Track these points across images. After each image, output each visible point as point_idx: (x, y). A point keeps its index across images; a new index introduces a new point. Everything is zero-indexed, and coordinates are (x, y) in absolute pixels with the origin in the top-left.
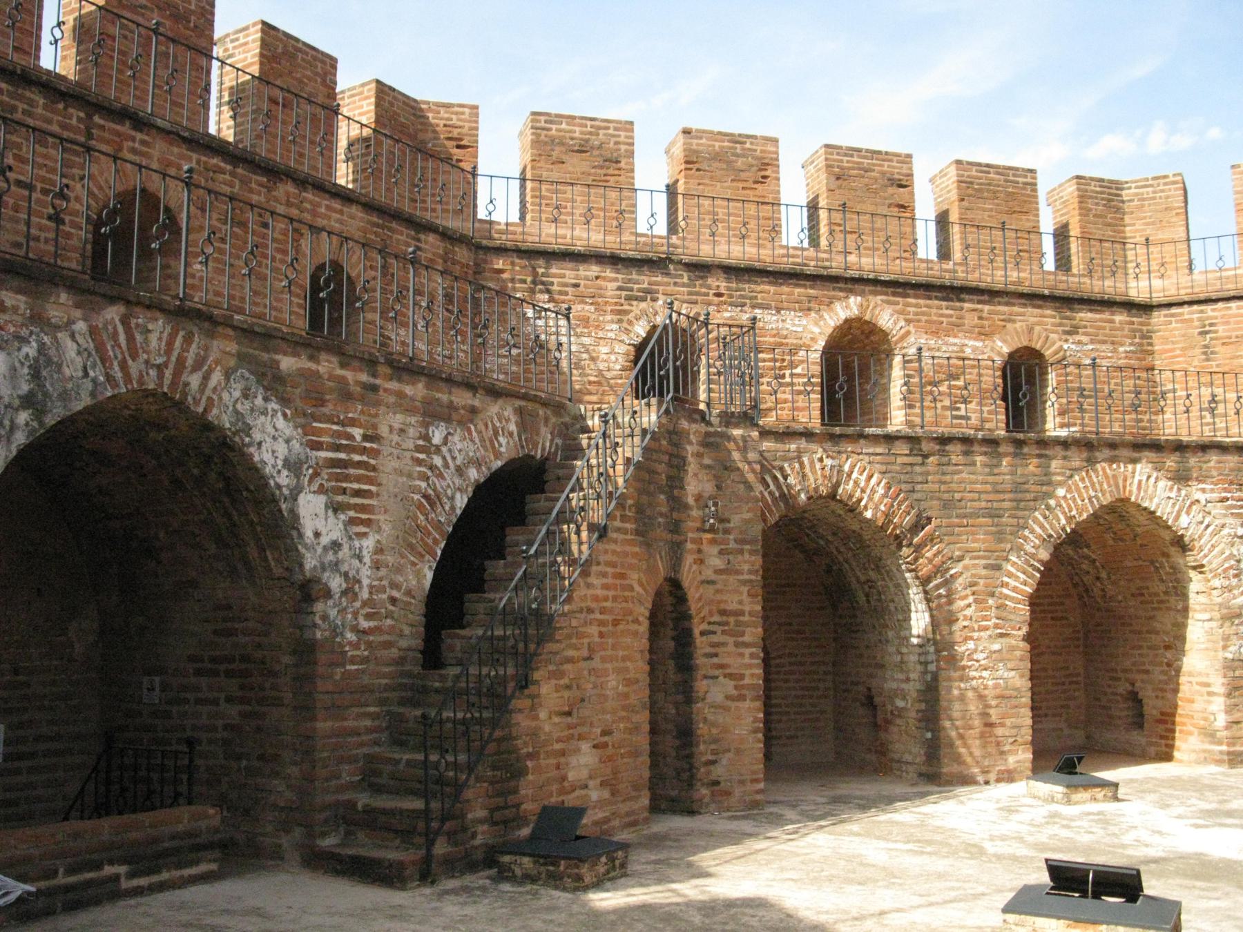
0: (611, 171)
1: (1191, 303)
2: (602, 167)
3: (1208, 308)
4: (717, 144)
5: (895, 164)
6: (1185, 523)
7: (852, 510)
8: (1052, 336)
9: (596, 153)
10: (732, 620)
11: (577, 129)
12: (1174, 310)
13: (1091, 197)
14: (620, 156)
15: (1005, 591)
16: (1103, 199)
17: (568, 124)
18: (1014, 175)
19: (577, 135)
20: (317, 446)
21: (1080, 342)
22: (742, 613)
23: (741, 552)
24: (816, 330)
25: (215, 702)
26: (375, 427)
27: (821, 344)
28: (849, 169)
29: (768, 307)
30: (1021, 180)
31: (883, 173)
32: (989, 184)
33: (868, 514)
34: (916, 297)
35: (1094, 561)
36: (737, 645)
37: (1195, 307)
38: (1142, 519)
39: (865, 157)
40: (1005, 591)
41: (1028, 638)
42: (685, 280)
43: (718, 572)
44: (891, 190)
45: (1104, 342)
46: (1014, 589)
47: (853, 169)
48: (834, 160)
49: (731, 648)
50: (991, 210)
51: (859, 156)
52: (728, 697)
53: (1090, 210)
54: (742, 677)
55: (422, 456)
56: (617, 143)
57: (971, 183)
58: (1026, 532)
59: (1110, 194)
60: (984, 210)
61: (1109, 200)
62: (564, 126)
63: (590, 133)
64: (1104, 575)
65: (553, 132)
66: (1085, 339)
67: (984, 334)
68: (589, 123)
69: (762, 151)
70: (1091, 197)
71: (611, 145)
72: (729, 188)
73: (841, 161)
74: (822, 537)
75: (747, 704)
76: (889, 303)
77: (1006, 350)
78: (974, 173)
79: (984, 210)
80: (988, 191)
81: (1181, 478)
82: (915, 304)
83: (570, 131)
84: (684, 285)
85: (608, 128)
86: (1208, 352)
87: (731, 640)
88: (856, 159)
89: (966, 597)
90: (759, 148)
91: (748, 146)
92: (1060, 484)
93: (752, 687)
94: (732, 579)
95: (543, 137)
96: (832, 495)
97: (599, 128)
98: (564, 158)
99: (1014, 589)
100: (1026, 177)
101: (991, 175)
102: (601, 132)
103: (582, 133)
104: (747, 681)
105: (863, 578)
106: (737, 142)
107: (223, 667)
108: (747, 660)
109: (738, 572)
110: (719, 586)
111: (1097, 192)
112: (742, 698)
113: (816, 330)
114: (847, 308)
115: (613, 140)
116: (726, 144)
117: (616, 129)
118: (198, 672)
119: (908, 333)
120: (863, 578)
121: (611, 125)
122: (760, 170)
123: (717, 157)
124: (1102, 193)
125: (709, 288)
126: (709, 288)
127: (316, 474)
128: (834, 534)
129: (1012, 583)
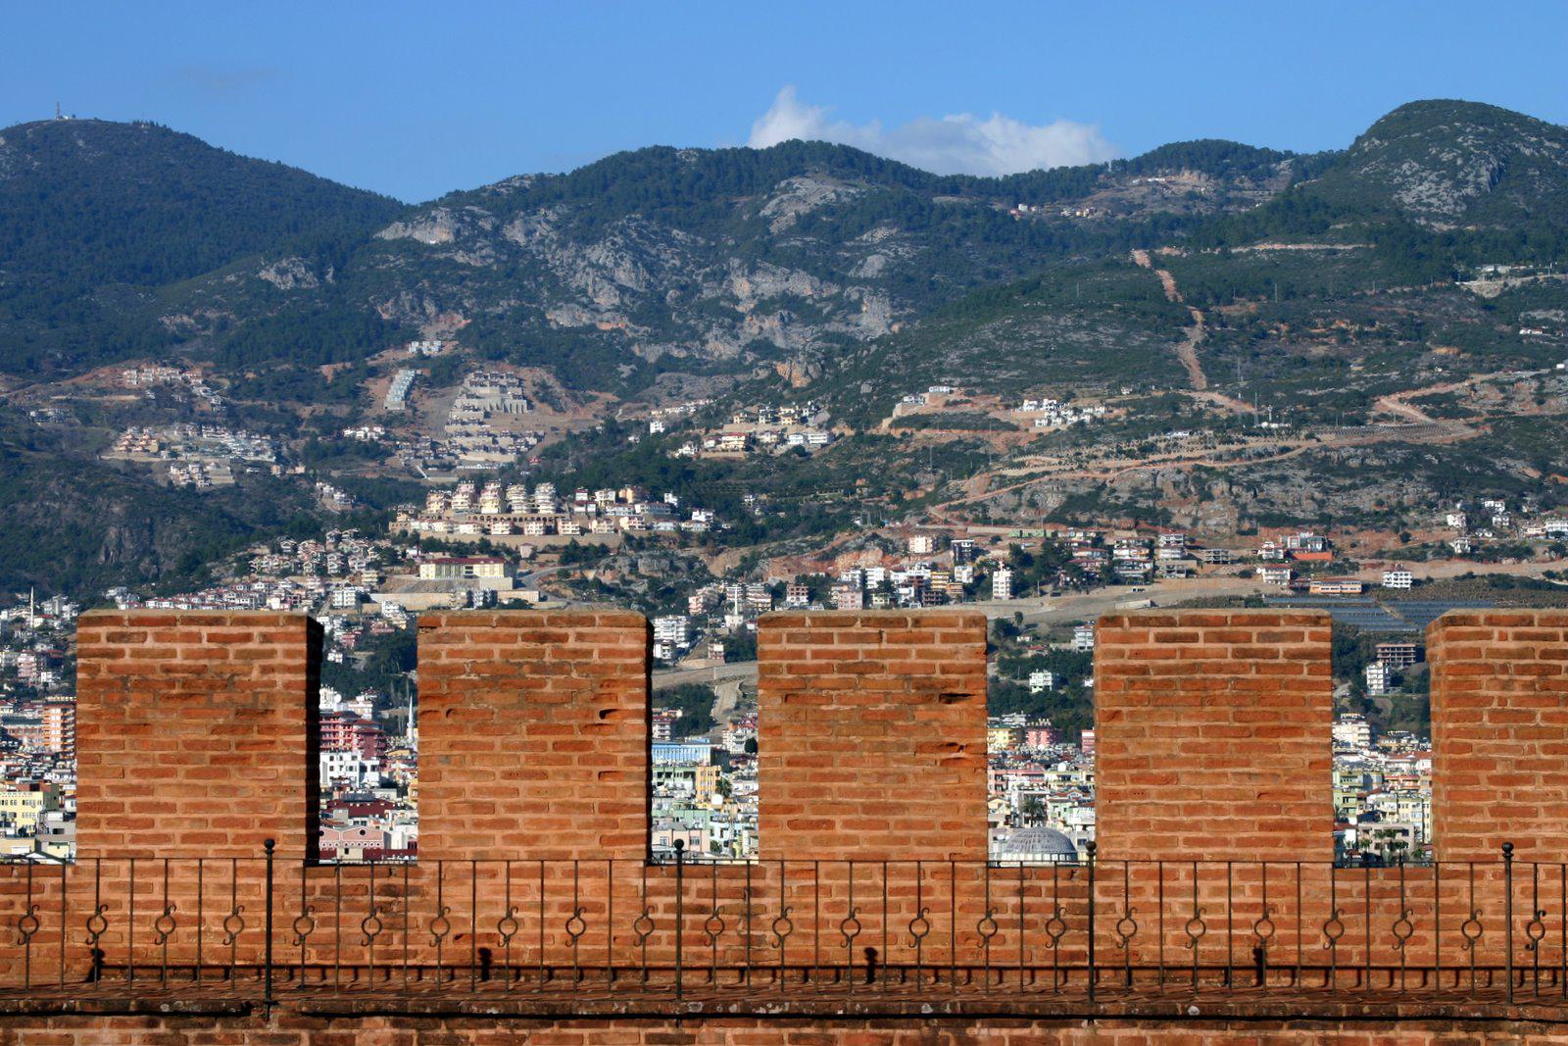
0: (256, 737)
2: (233, 730)
4: (497, 648)
5: (938, 646)
9: (219, 697)
11: (179, 647)
13: (1489, 669)
14: (271, 697)
16: (1523, 670)
17: (158, 637)
18: (1263, 637)
19: (178, 661)
28: (819, 670)
30: (1281, 647)
31: (905, 675)
32: (1193, 668)
39: (862, 638)
44: (923, 712)
47: (828, 669)
48: (782, 655)
50: (1194, 730)
51: (846, 638)
53: (1489, 700)
56: (265, 670)
57: (1144, 670)
59: (1545, 654)
60: (1174, 732)
61: (1544, 671)
62: (150, 644)
63: (209, 654)
65: (127, 660)
68: (205, 631)
69: (603, 653)
70: (1489, 669)
71: (255, 675)
72: (524, 746)
73: (800, 655)
78: (1152, 645)
79: (1174, 732)
80: (1186, 684)
83: (166, 654)
85: (248, 638)
88: (836, 646)
90: (596, 647)
91: (572, 644)
95: (103, 675)
97: (228, 639)
98: (152, 716)
100: (1299, 637)
101: (1200, 645)
102: (232, 648)
103: (188, 655)
106: (543, 638)
111: (1509, 654)
115: (257, 663)
116: (520, 645)
117: (266, 638)
121: (255, 631)
122: (596, 699)
123: (499, 679)
124: (1521, 654)
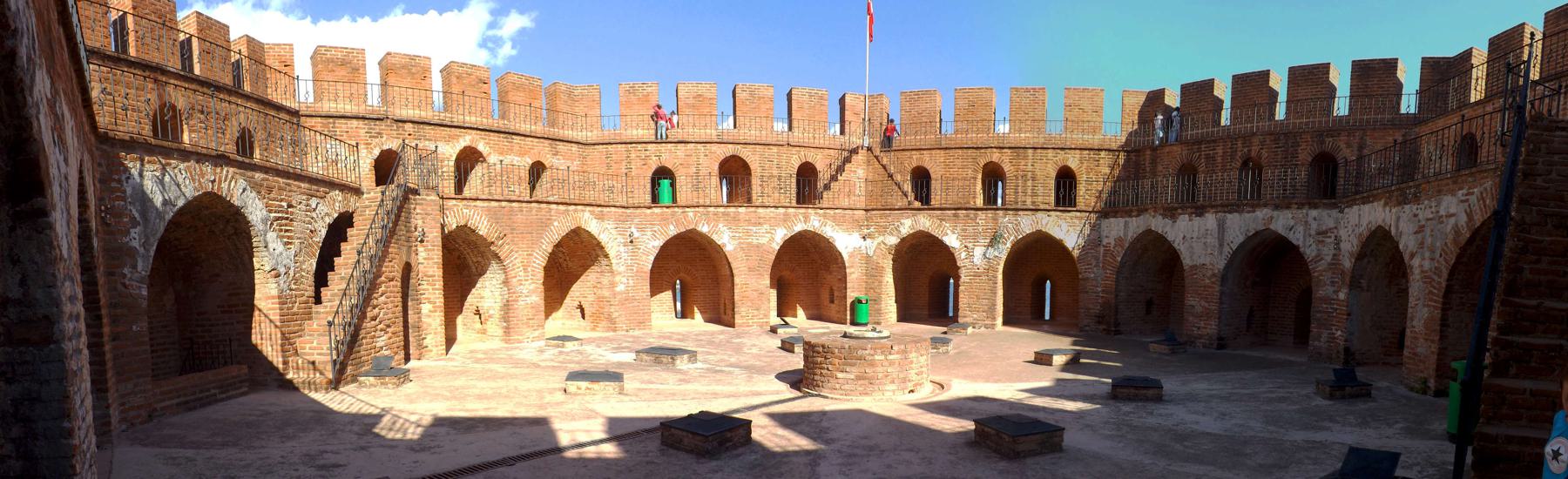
1: (603, 144)
3: (609, 147)
6: (603, 238)
7: (474, 231)
8: (548, 156)
10: (431, 279)
12: (596, 147)
15: (535, 265)
20: (270, 211)
21: (559, 159)
22: (435, 276)
23: (434, 250)
24: (452, 151)
25: (232, 324)
26: (291, 201)
27: (454, 158)
29: (431, 140)
31: (477, 77)
33: (481, 233)
34: (494, 136)
35: (564, 253)
36: (433, 289)
37: (605, 146)
38: (585, 235)
40: (535, 265)
41: (544, 283)
42: (395, 128)
43: (425, 259)
45: (568, 159)
46: (538, 264)
49: (431, 291)
52: (430, 311)
54: (435, 302)
55: (309, 213)
58: (543, 241)
64: (568, 259)
66: (561, 157)
67: (521, 155)
74: (457, 243)
75: (438, 314)
76: (483, 139)
77: (531, 162)
81: (601, 218)
82: (494, 136)
84: (394, 130)
86: (609, 166)
87: (430, 288)
89: (519, 268)
92: (555, 220)
93: (440, 307)
94: (430, 262)
96: (466, 226)
99: (538, 264)
104: (438, 304)
105: (475, 260)
107: (233, 309)
108: (438, 296)
109: (433, 259)
110: (425, 265)
112: (435, 311)
113: (452, 151)
114: (466, 140)
118: (223, 312)
119: (490, 153)
120: (475, 260)
125: (405, 131)
126: (405, 131)
127: (272, 224)
128: (463, 242)
129: (537, 262)
